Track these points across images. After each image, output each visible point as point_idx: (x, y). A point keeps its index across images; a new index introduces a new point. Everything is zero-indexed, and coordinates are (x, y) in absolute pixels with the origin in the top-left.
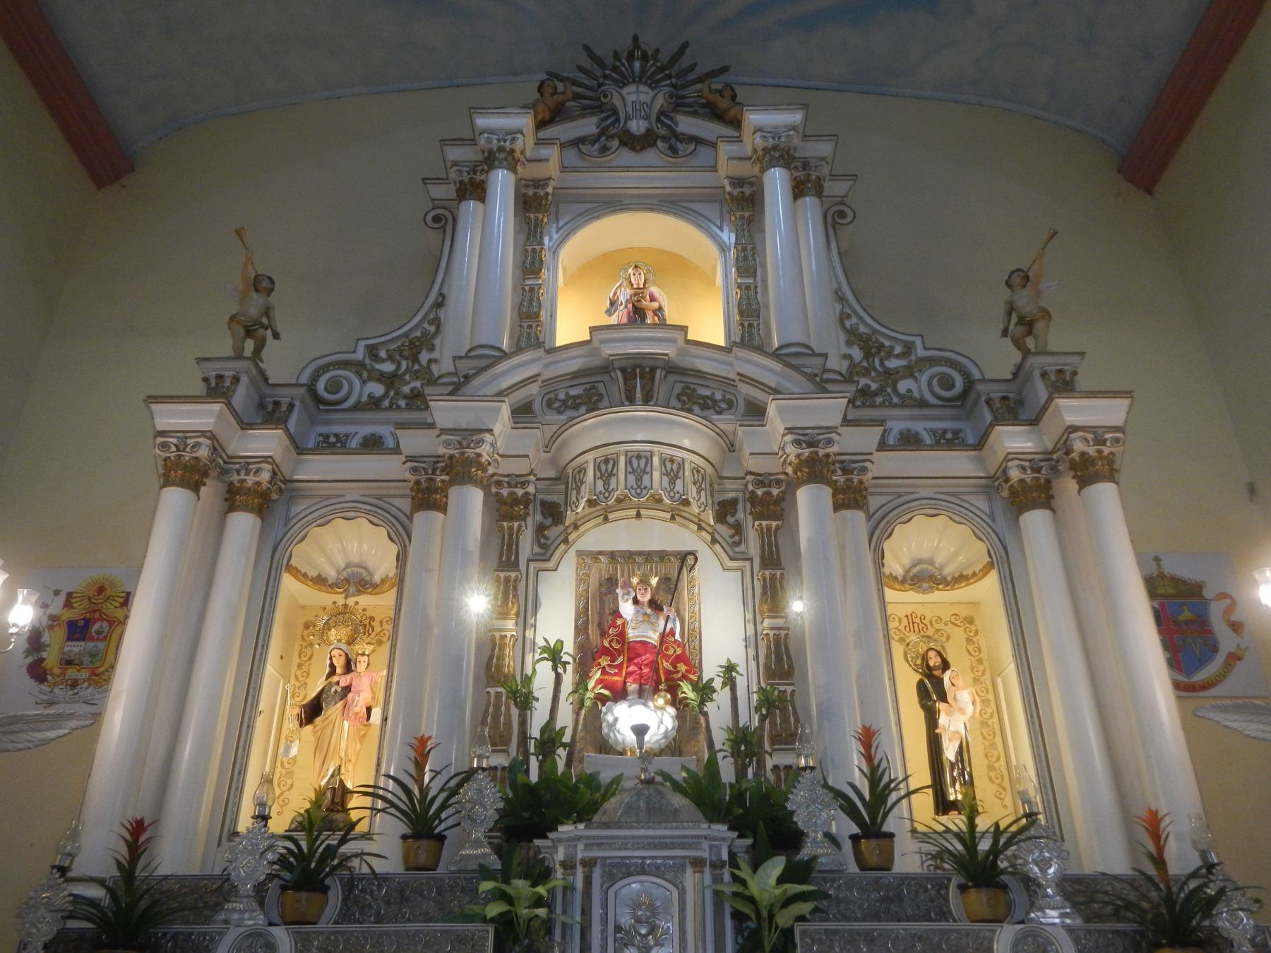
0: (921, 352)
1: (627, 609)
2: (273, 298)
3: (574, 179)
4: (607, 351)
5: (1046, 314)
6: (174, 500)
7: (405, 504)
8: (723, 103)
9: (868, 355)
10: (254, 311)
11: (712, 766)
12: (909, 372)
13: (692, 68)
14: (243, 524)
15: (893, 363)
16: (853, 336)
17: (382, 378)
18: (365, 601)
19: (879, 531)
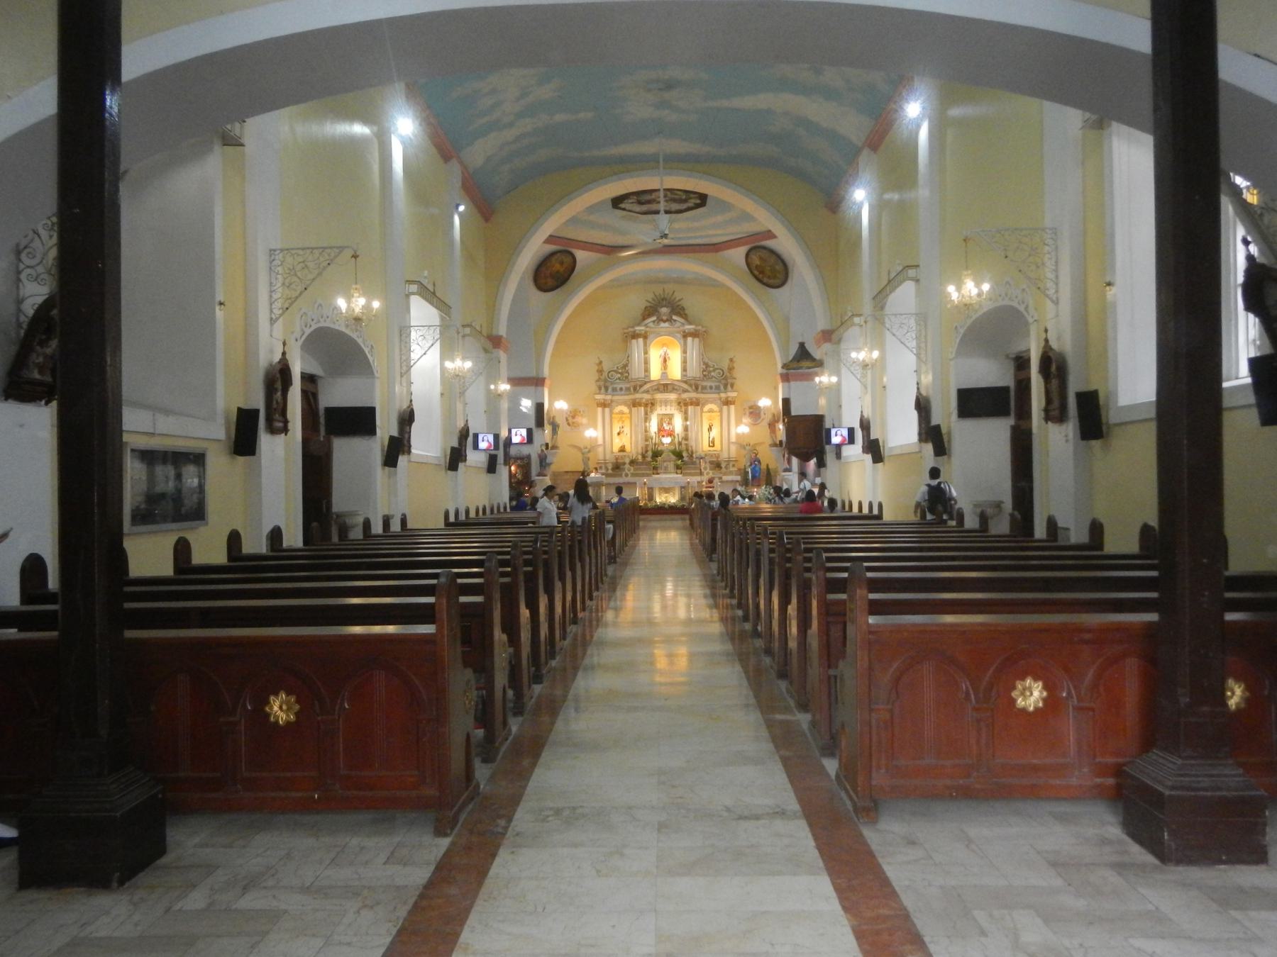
0: (716, 367)
1: (665, 425)
2: (604, 364)
3: (652, 330)
4: (662, 383)
5: (734, 368)
6: (600, 410)
7: (629, 403)
8: (682, 313)
9: (706, 367)
10: (601, 369)
11: (675, 449)
12: (714, 371)
13: (675, 299)
14: (607, 410)
15: (711, 369)
16: (704, 363)
17: (620, 373)
18: (624, 416)
19: (703, 405)
